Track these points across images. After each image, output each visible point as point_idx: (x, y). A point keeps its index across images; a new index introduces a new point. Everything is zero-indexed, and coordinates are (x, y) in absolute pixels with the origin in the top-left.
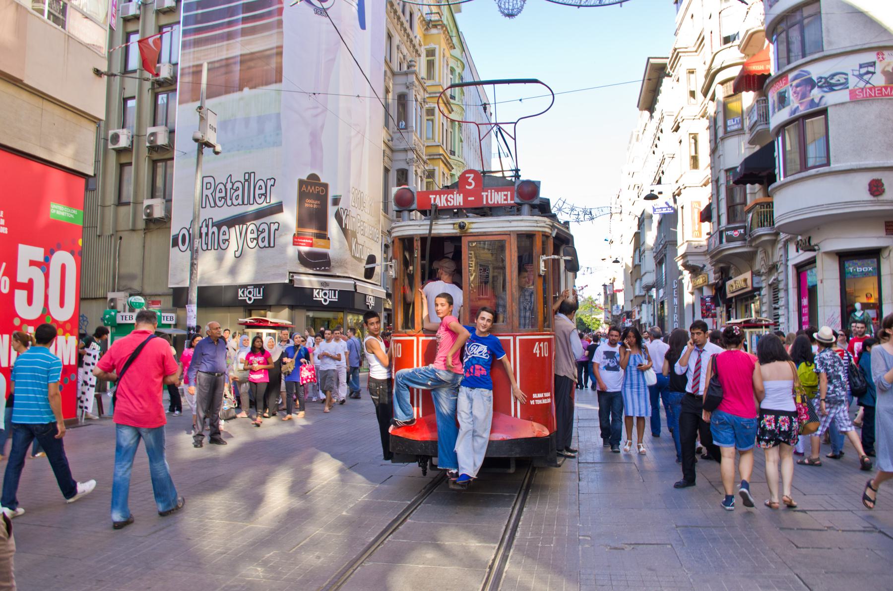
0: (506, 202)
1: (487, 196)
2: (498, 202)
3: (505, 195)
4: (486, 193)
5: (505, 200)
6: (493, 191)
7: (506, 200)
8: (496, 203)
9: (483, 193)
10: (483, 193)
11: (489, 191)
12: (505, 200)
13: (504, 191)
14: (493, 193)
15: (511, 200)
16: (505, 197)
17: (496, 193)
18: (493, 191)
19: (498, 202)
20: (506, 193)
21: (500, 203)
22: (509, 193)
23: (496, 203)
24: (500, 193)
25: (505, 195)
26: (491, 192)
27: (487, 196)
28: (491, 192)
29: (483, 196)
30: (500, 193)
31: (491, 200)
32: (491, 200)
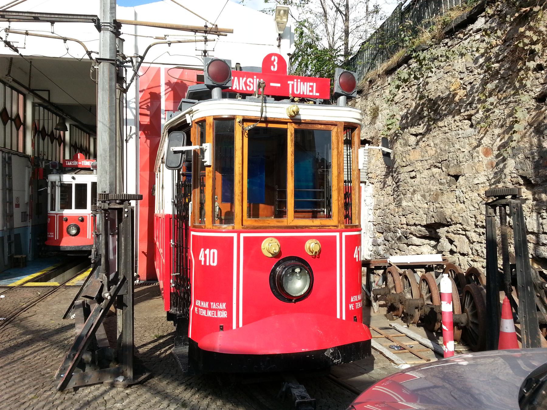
0: (311, 94)
1: (293, 85)
2: (303, 93)
3: (310, 86)
4: (292, 82)
5: (310, 91)
6: (299, 80)
7: (311, 91)
8: (302, 93)
9: (289, 82)
10: (289, 82)
11: (295, 80)
12: (310, 91)
13: (310, 82)
14: (299, 83)
15: (316, 92)
16: (310, 89)
17: (302, 83)
18: (299, 80)
19: (303, 93)
20: (311, 84)
21: (305, 94)
22: (315, 84)
23: (302, 93)
24: (305, 83)
25: (310, 86)
26: (297, 82)
27: (293, 85)
28: (297, 82)
29: (289, 84)
30: (305, 83)
31: (297, 90)
32: (297, 90)
